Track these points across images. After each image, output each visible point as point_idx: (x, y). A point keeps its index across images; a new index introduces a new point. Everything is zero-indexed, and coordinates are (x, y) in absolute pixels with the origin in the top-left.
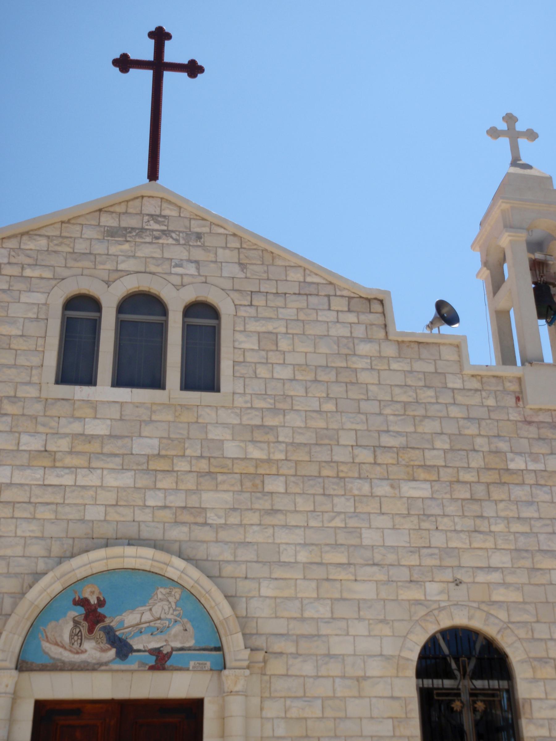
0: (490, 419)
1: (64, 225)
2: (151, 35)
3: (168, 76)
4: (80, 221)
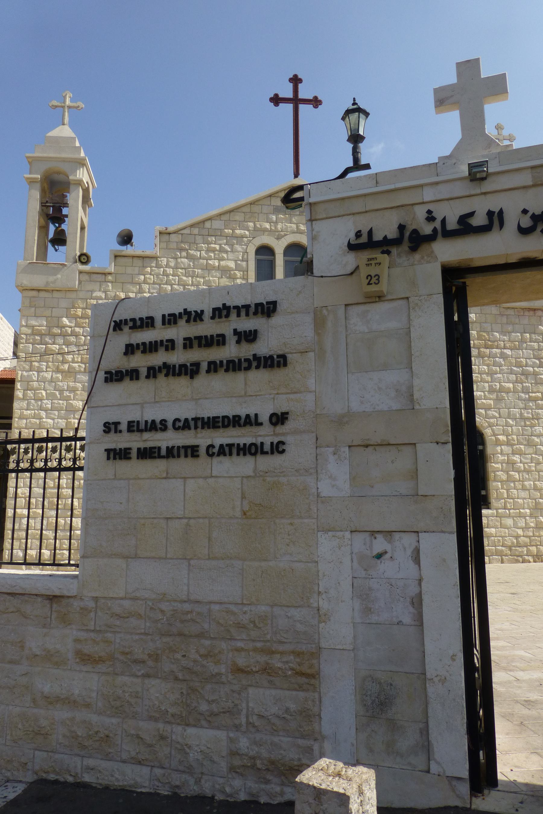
0: (481, 313)
1: (252, 206)
2: (291, 80)
3: (301, 107)
4: (261, 203)
